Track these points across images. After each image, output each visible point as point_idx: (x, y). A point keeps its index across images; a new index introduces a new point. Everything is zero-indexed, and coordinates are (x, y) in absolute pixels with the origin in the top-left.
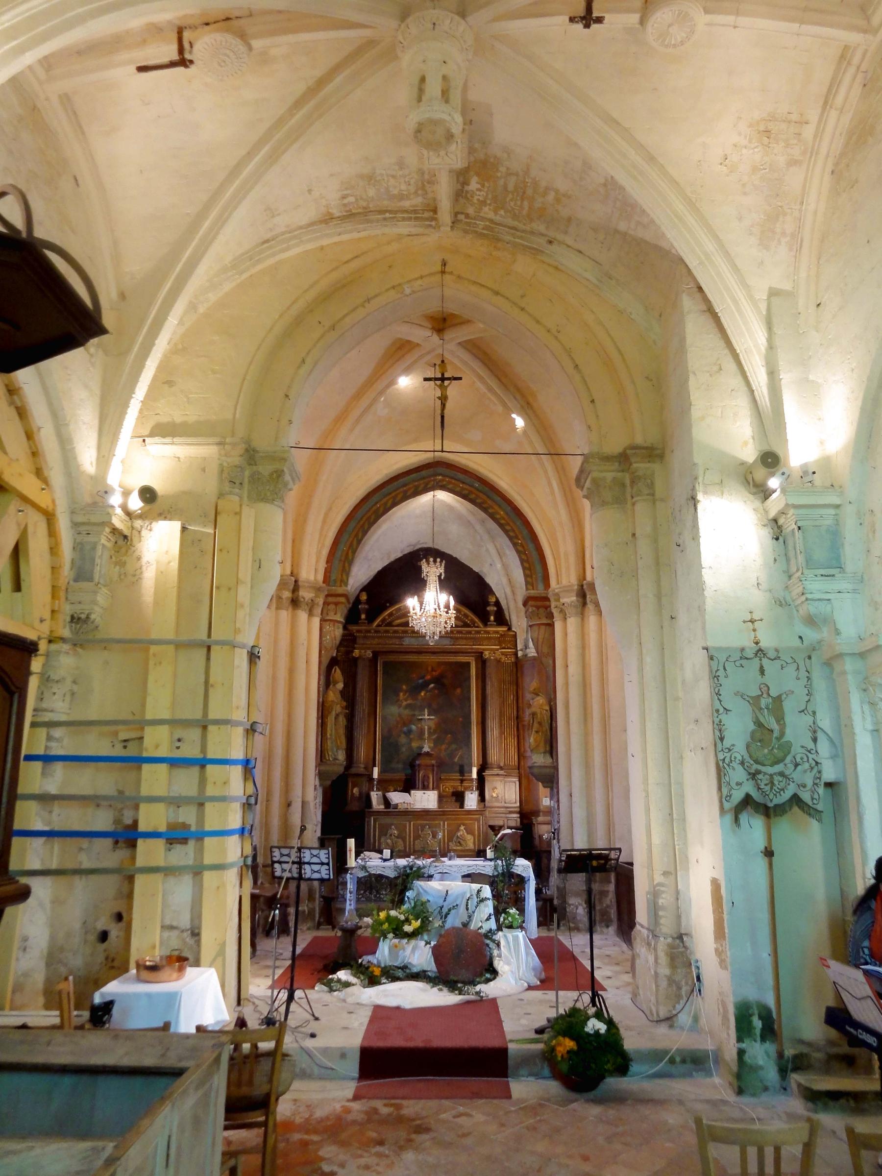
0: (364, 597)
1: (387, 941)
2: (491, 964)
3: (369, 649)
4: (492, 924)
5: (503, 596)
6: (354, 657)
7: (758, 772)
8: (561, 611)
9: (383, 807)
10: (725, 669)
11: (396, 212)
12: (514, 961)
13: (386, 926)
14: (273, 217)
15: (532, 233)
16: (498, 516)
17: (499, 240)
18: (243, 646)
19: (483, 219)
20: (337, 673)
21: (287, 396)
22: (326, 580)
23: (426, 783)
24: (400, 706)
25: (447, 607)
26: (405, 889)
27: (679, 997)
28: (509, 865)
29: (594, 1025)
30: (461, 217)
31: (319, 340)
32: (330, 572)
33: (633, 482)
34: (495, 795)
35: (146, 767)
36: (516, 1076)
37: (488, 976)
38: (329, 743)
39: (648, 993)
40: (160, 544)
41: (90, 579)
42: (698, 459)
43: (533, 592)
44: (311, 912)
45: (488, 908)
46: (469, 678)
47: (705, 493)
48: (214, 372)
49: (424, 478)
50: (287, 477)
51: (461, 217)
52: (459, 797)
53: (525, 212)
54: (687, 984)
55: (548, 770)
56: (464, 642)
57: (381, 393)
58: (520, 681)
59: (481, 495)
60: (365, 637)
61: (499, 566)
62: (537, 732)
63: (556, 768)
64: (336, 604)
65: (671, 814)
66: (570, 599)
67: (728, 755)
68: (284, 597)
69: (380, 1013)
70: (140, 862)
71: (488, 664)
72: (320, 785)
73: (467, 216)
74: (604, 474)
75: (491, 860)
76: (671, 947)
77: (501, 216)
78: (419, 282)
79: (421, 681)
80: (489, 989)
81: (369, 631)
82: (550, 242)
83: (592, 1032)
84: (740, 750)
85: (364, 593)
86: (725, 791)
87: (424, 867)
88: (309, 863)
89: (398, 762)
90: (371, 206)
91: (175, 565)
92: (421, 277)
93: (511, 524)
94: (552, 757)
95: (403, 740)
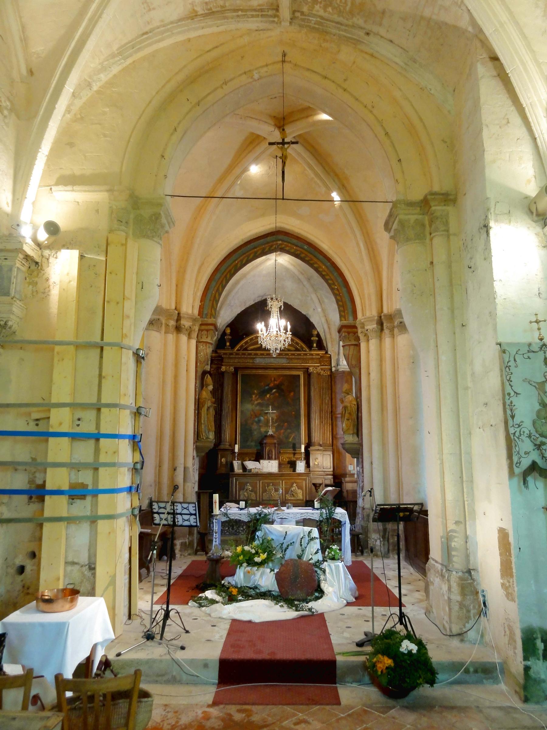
0: (228, 331)
1: (242, 568)
2: (319, 586)
3: (232, 366)
4: (319, 556)
5: (322, 330)
6: (221, 371)
7: (542, 443)
8: (365, 335)
10: (515, 360)
11: (246, 10)
12: (336, 584)
13: (241, 558)
14: (150, 10)
15: (353, 26)
16: (321, 270)
17: (327, 33)
18: (129, 348)
19: (315, 16)
20: (208, 379)
21: (163, 156)
22: (200, 313)
23: (270, 456)
24: (253, 404)
25: (286, 329)
26: (255, 530)
27: (468, 618)
28: (331, 513)
29: (407, 646)
30: (298, 14)
31: (187, 113)
32: (203, 308)
33: (431, 222)
34: (316, 463)
35: (51, 440)
36: (343, 682)
37: (317, 594)
38: (203, 426)
39: (441, 612)
40: (63, 269)
41: (7, 294)
42: (490, 193)
43: (345, 322)
44: (191, 543)
45: (316, 545)
46: (299, 386)
47: (496, 221)
48: (105, 136)
49: (268, 243)
50: (164, 220)
51: (298, 14)
52: (293, 465)
53: (348, 8)
54: (474, 607)
55: (355, 446)
56: (296, 361)
57: (238, 177)
58: (333, 387)
59: (309, 254)
61: (320, 310)
62: (348, 420)
63: (361, 445)
64: (207, 331)
65: (461, 477)
66: (372, 326)
67: (518, 430)
68: (170, 325)
69: (237, 627)
70: (47, 513)
71: (312, 376)
72: (197, 456)
73: (302, 13)
74: (409, 217)
75: (317, 509)
76: (461, 579)
77: (329, 13)
78: (265, 69)
79: (267, 388)
80: (317, 606)
81: (231, 354)
82: (368, 34)
83: (406, 652)
84: (528, 426)
85: (228, 328)
86: (515, 459)
87: (269, 514)
88: (181, 514)
89: (251, 442)
90: (227, 5)
91: (74, 284)
92: (267, 65)
93: (330, 275)
94: (358, 436)
95: (255, 427)
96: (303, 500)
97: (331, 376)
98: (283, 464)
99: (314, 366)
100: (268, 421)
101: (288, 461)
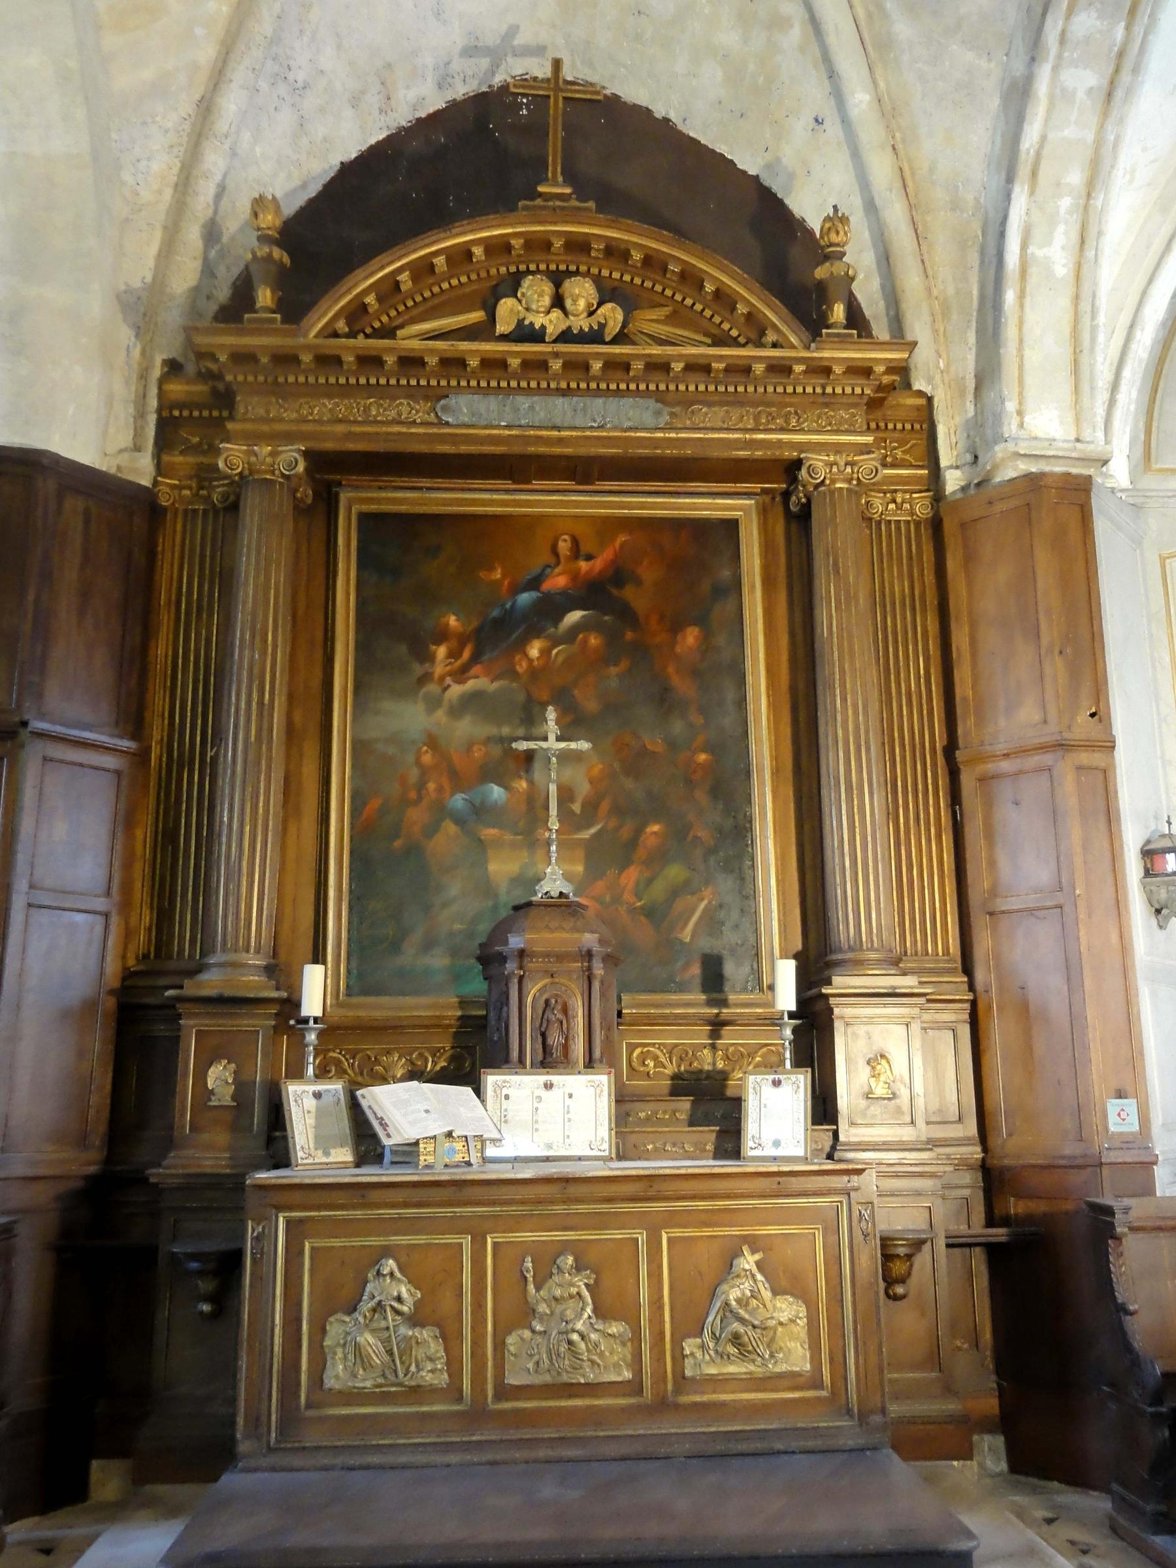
3: (289, 437)
9: (344, 1155)
23: (555, 1039)
24: (433, 704)
34: (880, 1090)
52: (713, 1104)
60: (276, 390)
79: (525, 598)
89: (428, 945)
96: (815, 1382)
97: (936, 525)
98: (641, 1098)
99: (838, 448)
100: (535, 808)
101: (676, 1077)
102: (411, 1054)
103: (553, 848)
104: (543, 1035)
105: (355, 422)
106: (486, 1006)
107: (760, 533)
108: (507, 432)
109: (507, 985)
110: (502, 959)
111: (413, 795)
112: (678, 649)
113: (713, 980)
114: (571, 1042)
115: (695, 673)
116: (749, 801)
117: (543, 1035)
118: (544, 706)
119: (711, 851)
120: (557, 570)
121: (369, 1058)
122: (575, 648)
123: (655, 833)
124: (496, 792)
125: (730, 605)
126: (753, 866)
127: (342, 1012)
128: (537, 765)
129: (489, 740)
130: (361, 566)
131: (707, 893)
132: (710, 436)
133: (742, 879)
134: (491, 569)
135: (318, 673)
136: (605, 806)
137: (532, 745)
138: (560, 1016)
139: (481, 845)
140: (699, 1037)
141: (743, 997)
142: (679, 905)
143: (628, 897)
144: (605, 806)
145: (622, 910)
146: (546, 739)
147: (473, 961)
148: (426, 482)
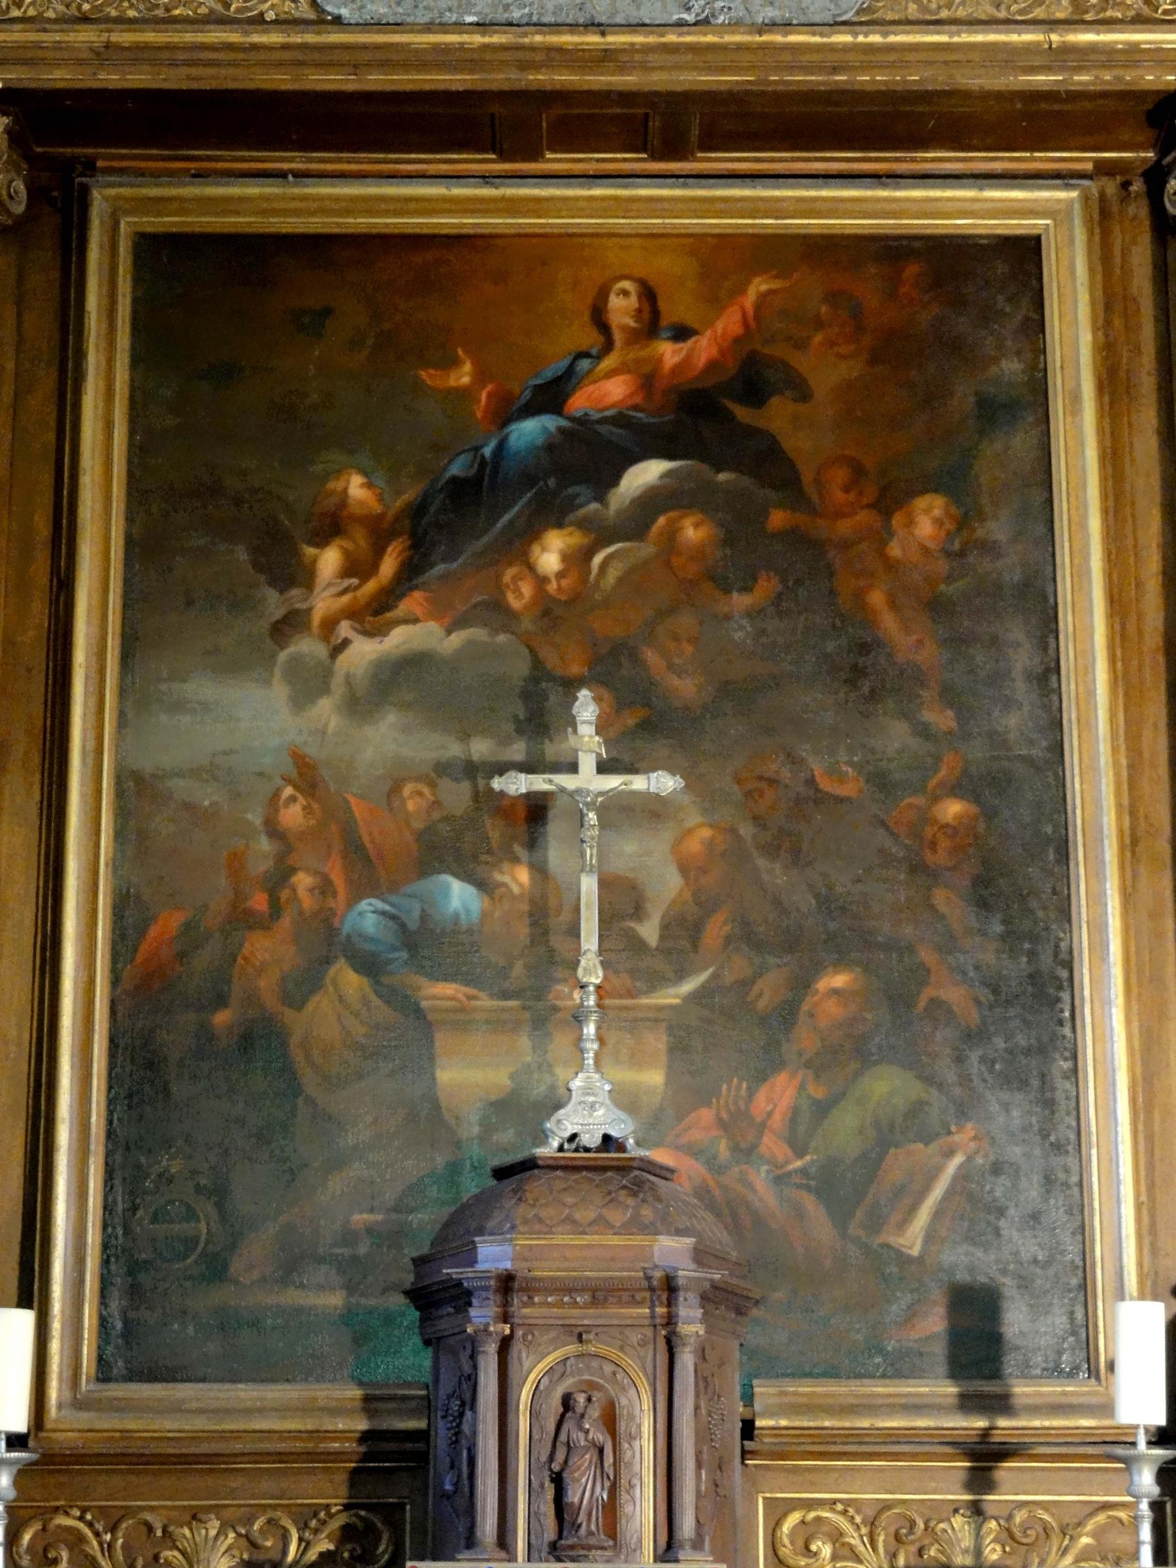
23: (585, 1489)
24: (309, 685)
46: (1036, 394)
79: (530, 431)
89: (291, 1264)
102: (250, 1521)
103: (590, 1029)
104: (558, 1480)
105: (121, 20)
106: (427, 1405)
107: (1091, 270)
108: (478, 39)
109: (473, 1357)
110: (460, 1297)
111: (259, 902)
112: (895, 550)
113: (977, 1348)
114: (624, 1497)
115: (937, 607)
116: (1065, 913)
117: (558, 1480)
118: (571, 686)
119: (974, 1036)
120: (608, 363)
121: (150, 1529)
122: (646, 550)
123: (836, 992)
124: (458, 896)
125: (1021, 442)
126: (1075, 1070)
127: (85, 1419)
128: (555, 828)
129: (442, 769)
130: (136, 361)
131: (964, 1136)
132: (965, 38)
133: (1050, 1104)
134: (453, 363)
135: (39, 610)
136: (717, 929)
137: (539, 783)
138: (599, 1436)
139: (419, 1022)
140: (946, 1484)
141: (1051, 1389)
142: (898, 1164)
143: (772, 1145)
144: (717, 929)
145: (760, 1178)
146: (573, 768)
147: (397, 1301)
148: (296, 161)
